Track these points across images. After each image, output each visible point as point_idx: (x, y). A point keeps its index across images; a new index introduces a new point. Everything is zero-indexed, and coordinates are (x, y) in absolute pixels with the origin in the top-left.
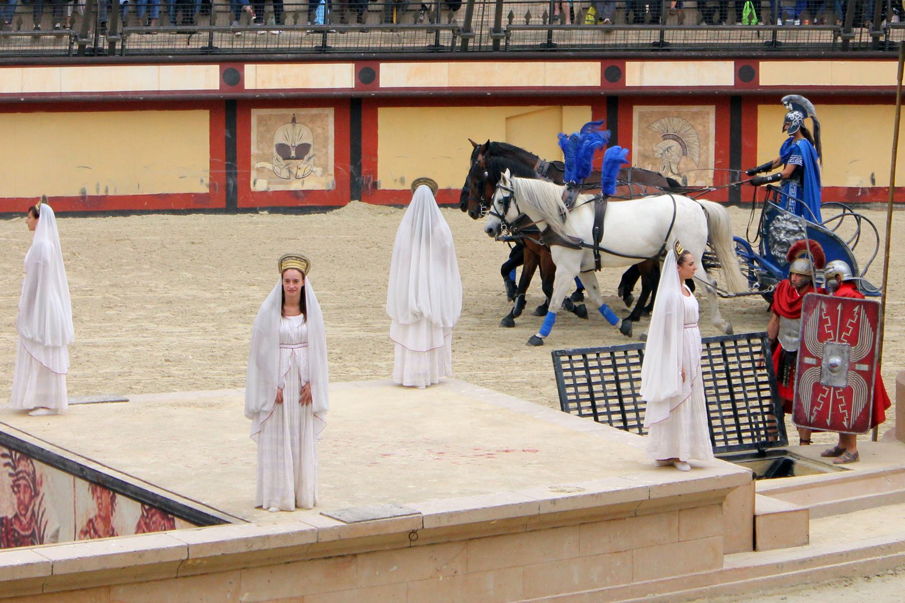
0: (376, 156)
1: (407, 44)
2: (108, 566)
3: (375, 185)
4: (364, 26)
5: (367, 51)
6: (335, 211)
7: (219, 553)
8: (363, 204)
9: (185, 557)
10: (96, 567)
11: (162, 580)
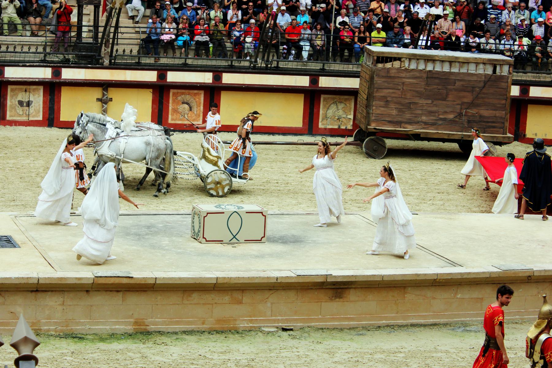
0: (526, 124)
1: (542, 80)
2: (405, 279)
3: (525, 135)
4: (525, 71)
5: (525, 81)
6: (507, 145)
7: (450, 278)
8: (519, 143)
9: (436, 278)
10: (400, 278)
11: (426, 286)
